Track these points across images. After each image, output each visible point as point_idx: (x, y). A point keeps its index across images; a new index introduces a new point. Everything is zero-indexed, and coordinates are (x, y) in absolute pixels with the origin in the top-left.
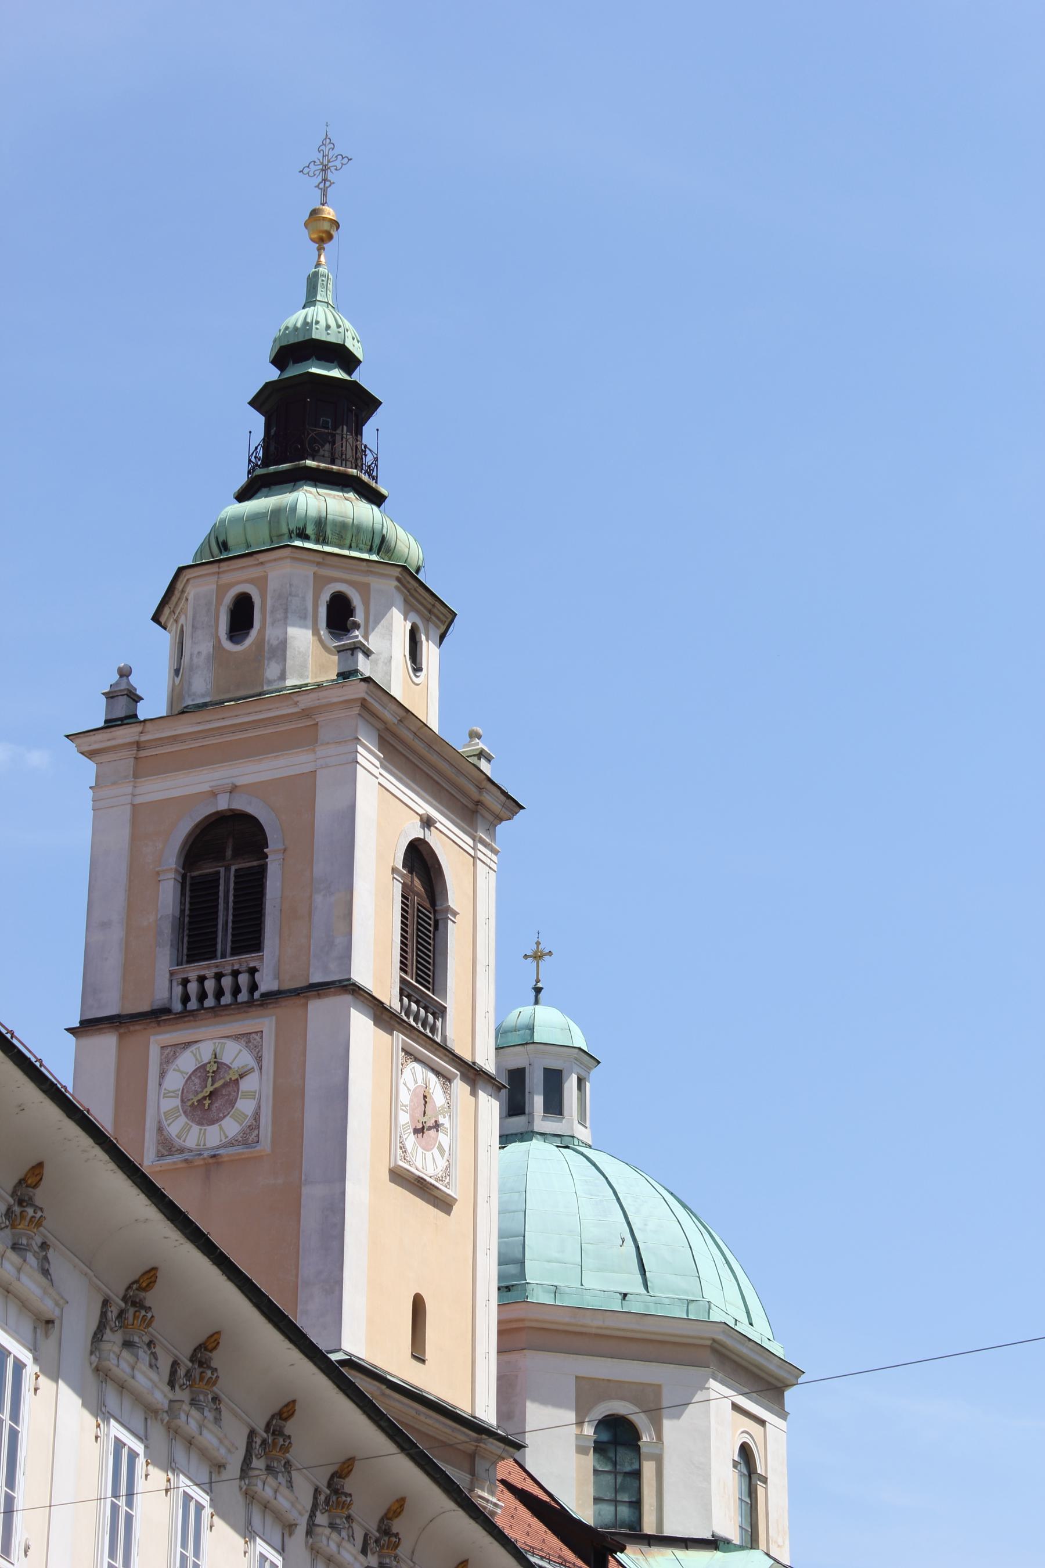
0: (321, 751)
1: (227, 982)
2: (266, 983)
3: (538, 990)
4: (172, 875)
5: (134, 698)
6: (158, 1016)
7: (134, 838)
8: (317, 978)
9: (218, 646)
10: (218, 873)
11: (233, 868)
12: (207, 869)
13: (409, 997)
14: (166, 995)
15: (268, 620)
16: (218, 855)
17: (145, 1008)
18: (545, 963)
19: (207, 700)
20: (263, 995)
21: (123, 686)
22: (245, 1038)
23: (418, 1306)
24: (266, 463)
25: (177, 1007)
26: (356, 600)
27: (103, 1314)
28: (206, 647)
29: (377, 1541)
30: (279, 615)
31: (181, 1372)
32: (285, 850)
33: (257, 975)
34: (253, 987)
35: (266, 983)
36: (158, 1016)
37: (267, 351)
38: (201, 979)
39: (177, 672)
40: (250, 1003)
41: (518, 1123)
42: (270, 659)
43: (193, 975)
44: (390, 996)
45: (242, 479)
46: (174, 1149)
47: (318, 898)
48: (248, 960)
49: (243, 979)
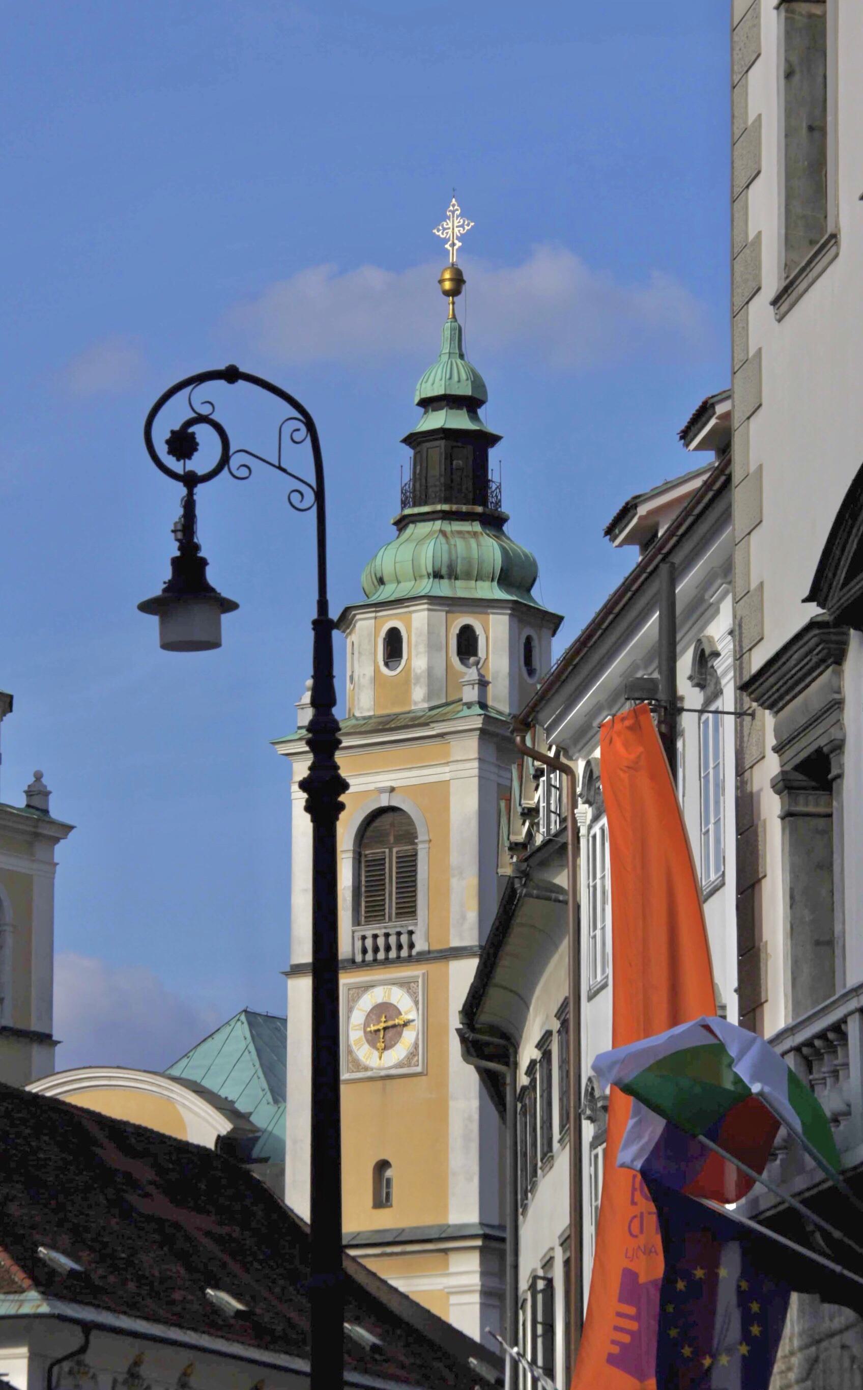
1: (393, 940)
2: (420, 946)
4: (350, 855)
8: (455, 943)
9: (377, 670)
10: (384, 852)
11: (395, 850)
14: (350, 949)
15: (413, 653)
19: (371, 713)
20: (419, 954)
22: (405, 984)
25: (359, 958)
26: (479, 630)
28: (369, 671)
32: (430, 841)
33: (414, 937)
34: (411, 946)
35: (418, 948)
38: (375, 937)
42: (415, 684)
43: (369, 934)
45: (396, 513)
46: (361, 1067)
48: (406, 924)
49: (404, 939)
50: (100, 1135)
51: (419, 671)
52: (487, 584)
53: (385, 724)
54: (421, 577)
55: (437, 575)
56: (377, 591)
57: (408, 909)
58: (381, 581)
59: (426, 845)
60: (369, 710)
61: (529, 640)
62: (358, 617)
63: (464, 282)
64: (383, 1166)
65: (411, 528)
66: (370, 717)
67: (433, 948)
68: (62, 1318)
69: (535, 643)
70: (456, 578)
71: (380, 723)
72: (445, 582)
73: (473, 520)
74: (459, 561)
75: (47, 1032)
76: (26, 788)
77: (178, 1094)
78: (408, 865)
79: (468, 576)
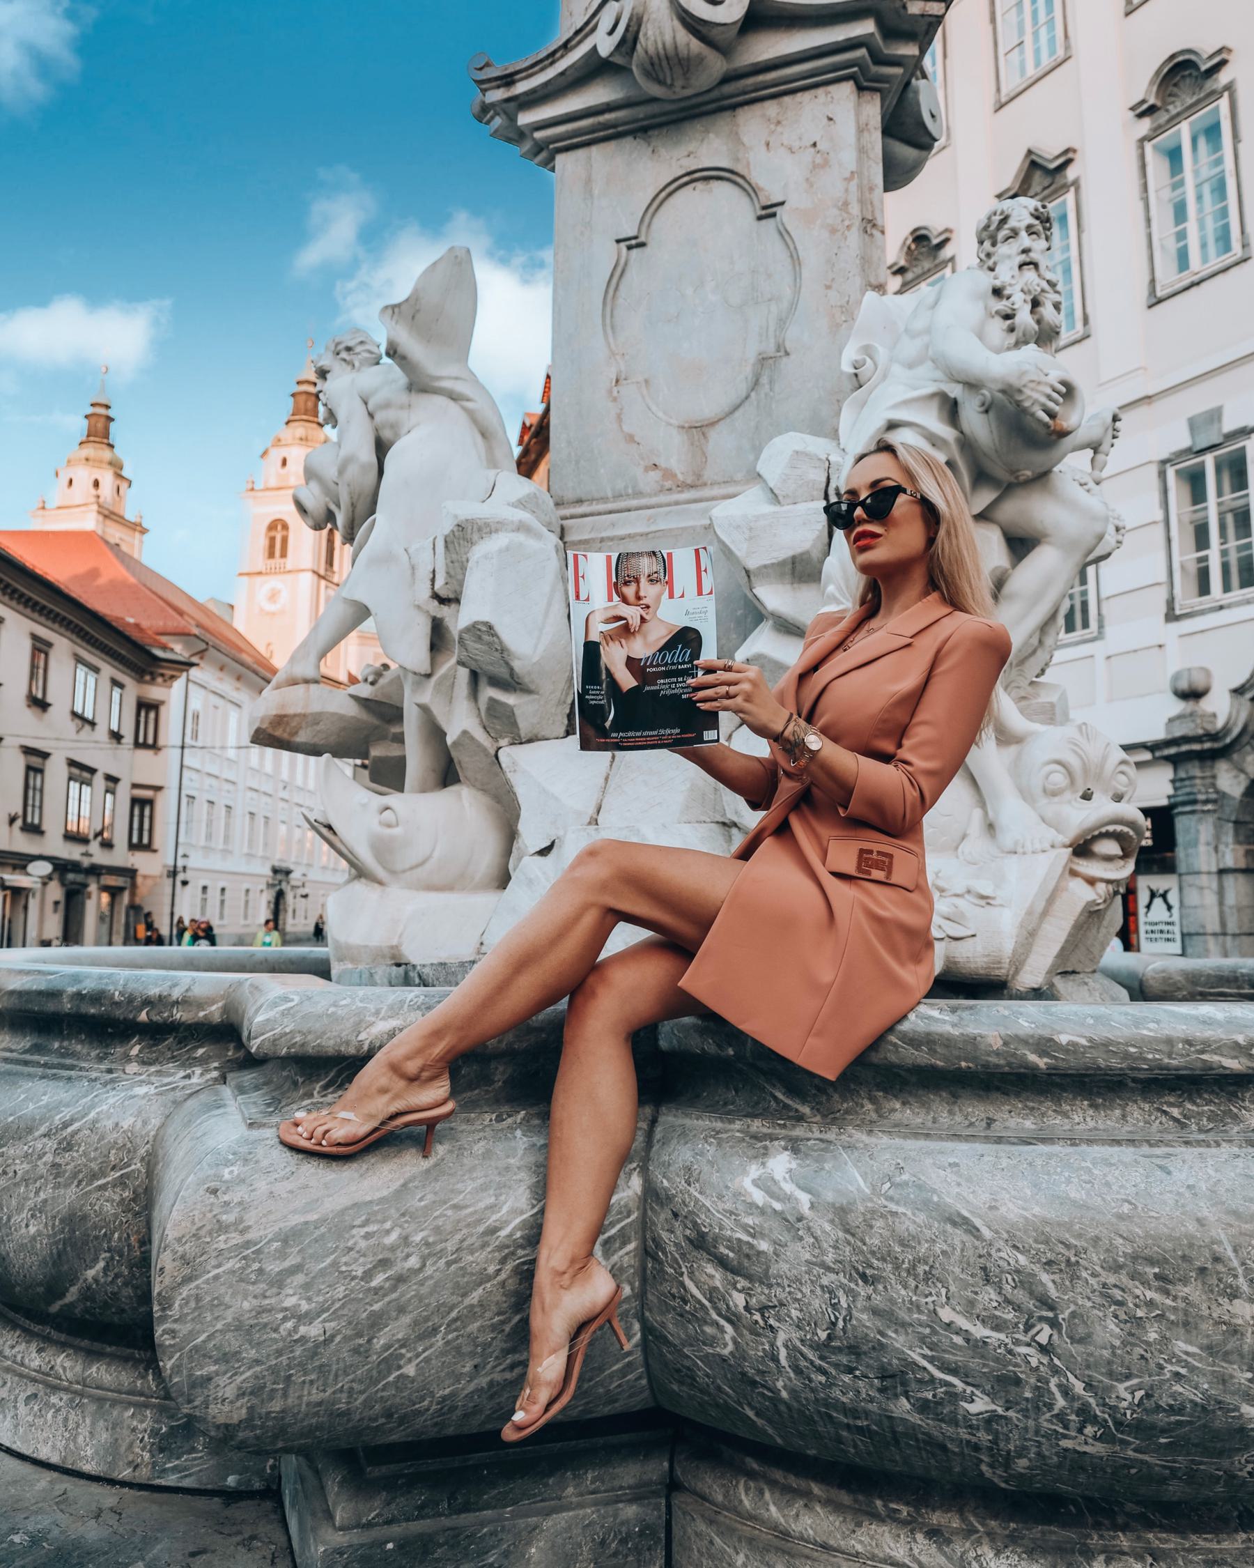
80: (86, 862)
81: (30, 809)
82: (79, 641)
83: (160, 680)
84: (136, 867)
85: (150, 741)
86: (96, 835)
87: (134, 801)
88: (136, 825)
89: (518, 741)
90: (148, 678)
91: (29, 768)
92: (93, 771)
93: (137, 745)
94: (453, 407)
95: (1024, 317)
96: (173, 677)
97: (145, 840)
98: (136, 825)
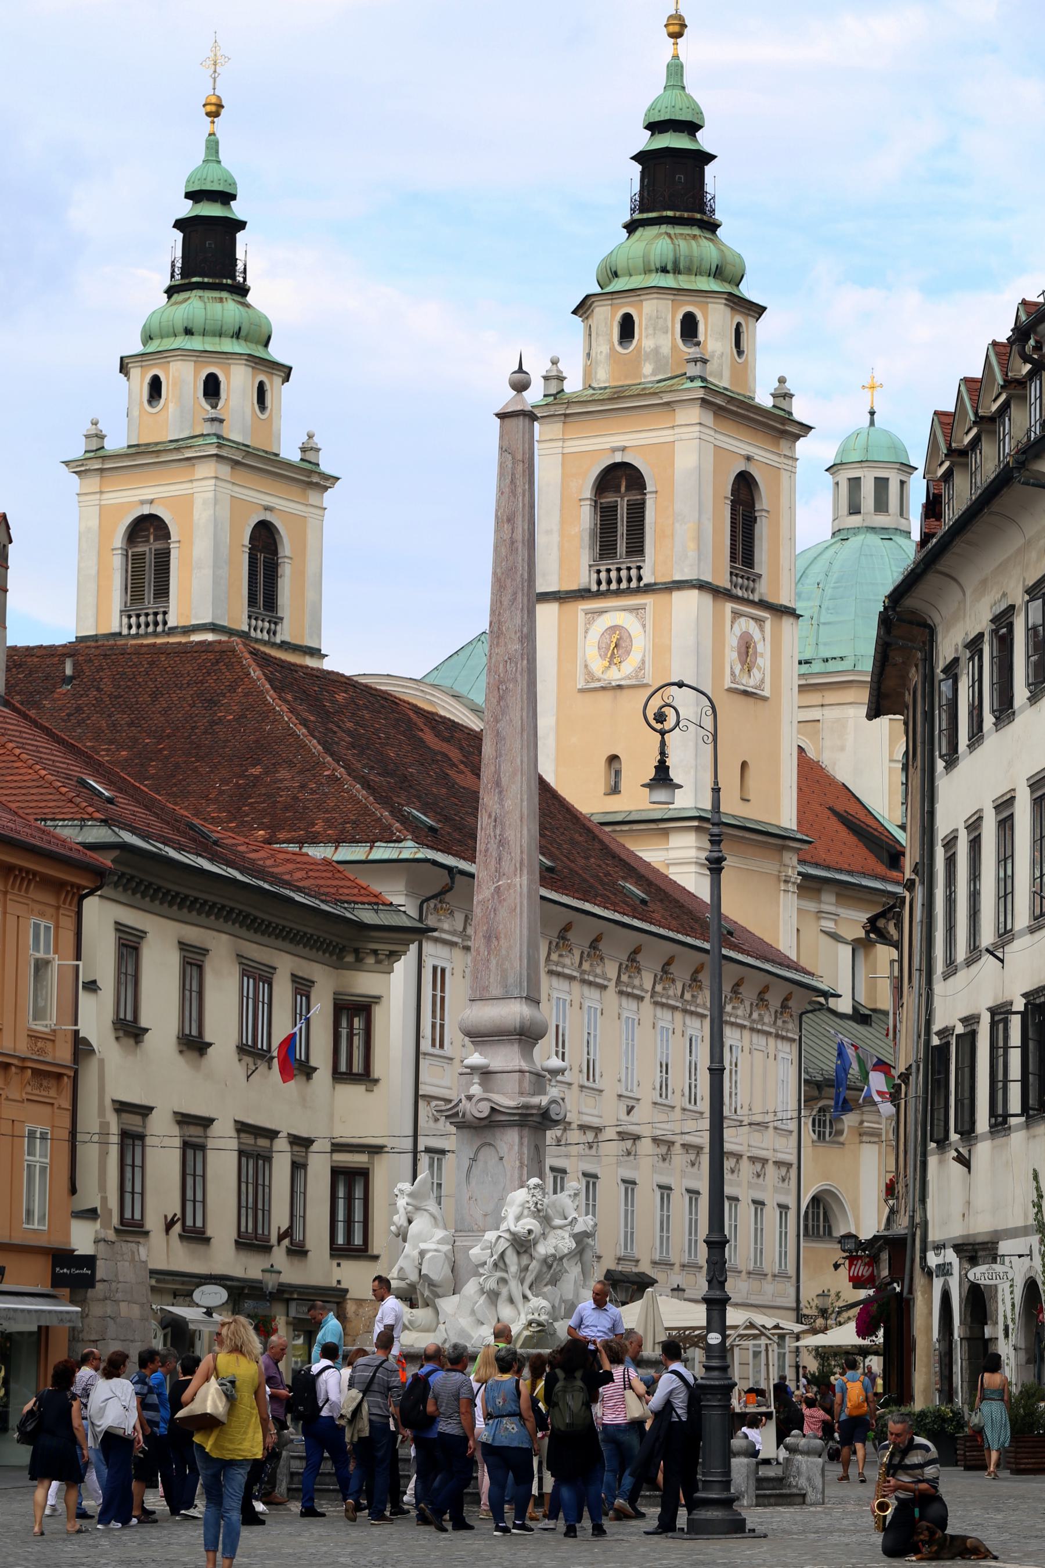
0: (677, 430)
3: (872, 413)
5: (561, 379)
6: (583, 594)
7: (563, 474)
9: (612, 349)
11: (626, 499)
12: (609, 499)
13: (737, 575)
14: (587, 580)
16: (618, 490)
17: (574, 587)
18: (877, 392)
20: (646, 585)
21: (554, 373)
23: (744, 765)
24: (641, 211)
25: (594, 588)
26: (699, 317)
27: (550, 948)
28: (605, 349)
29: (690, 986)
30: (651, 331)
31: (585, 955)
34: (640, 579)
36: (583, 594)
37: (641, 123)
38: (608, 571)
39: (589, 355)
40: (638, 591)
41: (855, 521)
43: (603, 568)
44: (723, 581)
45: (627, 218)
47: (677, 525)
50: (419, 722)
51: (648, 350)
52: (704, 279)
53: (618, 395)
54: (650, 271)
55: (664, 270)
56: (610, 281)
57: (636, 548)
58: (616, 274)
59: (654, 495)
60: (604, 382)
61: (739, 325)
62: (596, 304)
63: (686, 26)
64: (613, 759)
65: (640, 232)
66: (605, 388)
67: (659, 581)
68: (434, 863)
69: (744, 328)
70: (679, 273)
71: (615, 393)
72: (671, 276)
73: (693, 225)
74: (682, 258)
75: (317, 646)
76: (301, 445)
77: (438, 698)
78: (637, 514)
79: (689, 271)
80: (271, 1282)
81: (189, 1206)
82: (243, 932)
83: (370, 960)
84: (343, 1286)
85: (357, 1067)
86: (281, 1238)
87: (337, 1173)
88: (341, 1216)
89: (439, 1297)
90: (350, 958)
91: (186, 1145)
92: (272, 1134)
93: (339, 1076)
94: (425, 1213)
95: (532, 1208)
96: (394, 956)
97: (358, 1240)
98: (341, 1216)
